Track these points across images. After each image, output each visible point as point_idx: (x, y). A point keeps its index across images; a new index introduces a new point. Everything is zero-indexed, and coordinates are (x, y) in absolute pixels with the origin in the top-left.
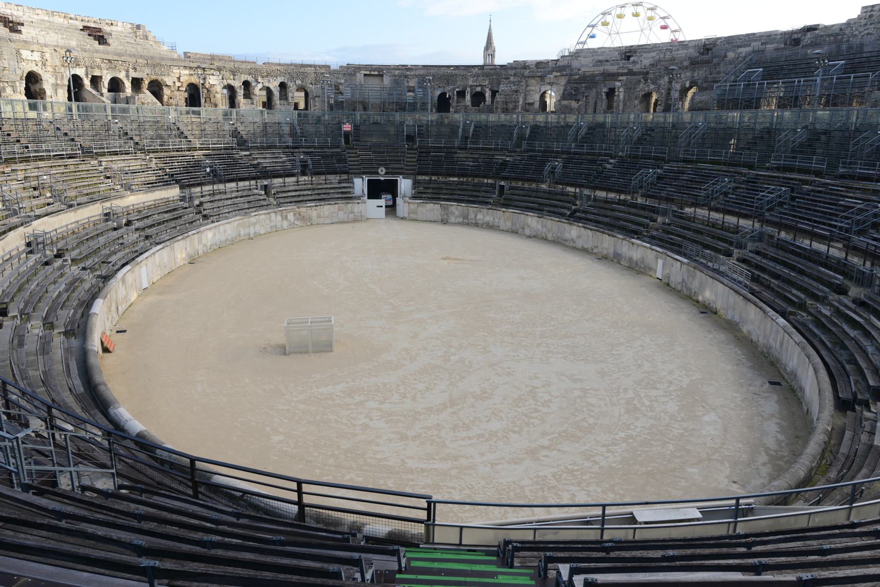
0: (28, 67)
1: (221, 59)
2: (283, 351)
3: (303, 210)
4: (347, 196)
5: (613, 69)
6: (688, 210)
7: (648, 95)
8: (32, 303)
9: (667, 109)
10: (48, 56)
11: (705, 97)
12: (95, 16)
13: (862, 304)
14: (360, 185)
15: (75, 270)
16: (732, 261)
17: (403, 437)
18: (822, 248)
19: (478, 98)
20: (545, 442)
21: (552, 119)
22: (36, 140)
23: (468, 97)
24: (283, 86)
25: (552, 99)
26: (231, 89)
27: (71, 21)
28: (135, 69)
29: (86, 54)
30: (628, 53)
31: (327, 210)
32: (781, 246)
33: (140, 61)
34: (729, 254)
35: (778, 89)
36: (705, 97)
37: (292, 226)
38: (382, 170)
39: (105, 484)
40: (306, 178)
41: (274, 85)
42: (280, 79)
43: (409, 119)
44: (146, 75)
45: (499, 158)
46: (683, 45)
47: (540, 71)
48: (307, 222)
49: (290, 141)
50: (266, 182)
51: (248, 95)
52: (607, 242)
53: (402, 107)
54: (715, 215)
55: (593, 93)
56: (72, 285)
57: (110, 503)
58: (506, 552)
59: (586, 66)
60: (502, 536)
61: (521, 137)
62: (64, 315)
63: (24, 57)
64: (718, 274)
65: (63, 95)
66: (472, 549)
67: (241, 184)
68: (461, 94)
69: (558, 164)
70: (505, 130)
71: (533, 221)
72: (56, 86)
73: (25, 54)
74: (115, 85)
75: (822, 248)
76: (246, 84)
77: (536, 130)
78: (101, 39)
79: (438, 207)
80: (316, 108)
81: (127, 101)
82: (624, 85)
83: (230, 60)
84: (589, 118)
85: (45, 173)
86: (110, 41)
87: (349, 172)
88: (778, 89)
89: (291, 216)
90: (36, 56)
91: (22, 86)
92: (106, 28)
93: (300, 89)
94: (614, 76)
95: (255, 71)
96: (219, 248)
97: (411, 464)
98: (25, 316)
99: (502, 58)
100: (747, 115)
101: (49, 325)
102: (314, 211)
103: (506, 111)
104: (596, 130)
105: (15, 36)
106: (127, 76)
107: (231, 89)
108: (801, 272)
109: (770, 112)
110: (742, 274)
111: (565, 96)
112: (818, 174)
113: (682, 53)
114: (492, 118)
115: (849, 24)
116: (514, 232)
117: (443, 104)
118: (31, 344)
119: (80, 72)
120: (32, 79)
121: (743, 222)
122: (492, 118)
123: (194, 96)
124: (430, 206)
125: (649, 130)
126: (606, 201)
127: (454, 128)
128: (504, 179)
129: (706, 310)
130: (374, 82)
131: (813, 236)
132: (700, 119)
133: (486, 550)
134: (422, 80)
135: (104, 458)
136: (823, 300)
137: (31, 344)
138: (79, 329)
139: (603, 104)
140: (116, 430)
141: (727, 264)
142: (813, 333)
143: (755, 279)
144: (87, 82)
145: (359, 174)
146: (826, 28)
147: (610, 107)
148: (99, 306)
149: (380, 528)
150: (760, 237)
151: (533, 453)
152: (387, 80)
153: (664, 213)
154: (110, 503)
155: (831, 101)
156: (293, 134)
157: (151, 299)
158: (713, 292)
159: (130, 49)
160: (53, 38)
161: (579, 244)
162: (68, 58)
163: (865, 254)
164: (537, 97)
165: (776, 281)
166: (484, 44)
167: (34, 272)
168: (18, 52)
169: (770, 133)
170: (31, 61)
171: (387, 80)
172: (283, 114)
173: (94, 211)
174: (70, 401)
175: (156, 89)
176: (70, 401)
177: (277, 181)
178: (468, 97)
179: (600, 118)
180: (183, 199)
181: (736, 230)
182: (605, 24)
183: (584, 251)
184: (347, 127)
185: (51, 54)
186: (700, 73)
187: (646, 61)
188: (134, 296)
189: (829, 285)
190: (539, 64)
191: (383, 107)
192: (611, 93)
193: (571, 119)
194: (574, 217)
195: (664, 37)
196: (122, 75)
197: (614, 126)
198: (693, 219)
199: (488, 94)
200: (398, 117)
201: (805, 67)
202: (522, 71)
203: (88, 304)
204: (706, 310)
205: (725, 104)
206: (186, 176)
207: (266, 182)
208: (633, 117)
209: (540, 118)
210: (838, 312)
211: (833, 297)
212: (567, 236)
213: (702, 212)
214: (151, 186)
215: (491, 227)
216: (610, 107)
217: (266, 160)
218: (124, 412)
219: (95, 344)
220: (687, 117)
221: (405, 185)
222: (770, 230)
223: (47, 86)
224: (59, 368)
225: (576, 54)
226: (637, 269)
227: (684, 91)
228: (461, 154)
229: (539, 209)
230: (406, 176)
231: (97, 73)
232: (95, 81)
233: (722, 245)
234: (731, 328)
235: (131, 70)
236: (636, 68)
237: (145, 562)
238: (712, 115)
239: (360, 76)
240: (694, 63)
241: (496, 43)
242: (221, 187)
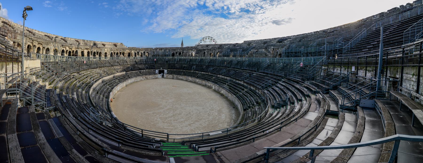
0: (105, 52)
1: (134, 48)
4: (155, 74)
5: (205, 48)
7: (211, 54)
8: (102, 92)
9: (214, 56)
11: (221, 54)
12: (115, 42)
13: (246, 92)
14: (157, 71)
15: (108, 86)
16: (226, 85)
17: (164, 122)
18: (240, 82)
19: (180, 54)
20: (192, 122)
21: (194, 58)
22: (105, 63)
25: (194, 54)
26: (135, 53)
30: (207, 46)
31: (151, 76)
32: (234, 82)
35: (232, 54)
36: (221, 54)
37: (144, 79)
38: (161, 68)
39: (110, 125)
43: (167, 58)
44: (122, 51)
45: (184, 66)
46: (217, 45)
47: (192, 48)
48: (147, 78)
49: (145, 63)
51: (138, 54)
52: (204, 82)
53: (165, 56)
55: (201, 53)
56: (107, 89)
57: (111, 129)
58: (183, 143)
59: (200, 48)
60: (182, 140)
61: (188, 61)
62: (106, 94)
64: (224, 88)
65: (110, 56)
66: (176, 143)
69: (195, 67)
70: (185, 60)
71: (190, 78)
74: (117, 54)
75: (240, 82)
76: (138, 52)
77: (190, 60)
78: (116, 46)
80: (150, 56)
83: (136, 48)
84: (200, 58)
85: (106, 69)
87: (155, 69)
88: (232, 54)
93: (147, 53)
96: (131, 84)
97: (165, 127)
98: (101, 94)
99: (184, 46)
100: (228, 58)
101: (103, 96)
102: (148, 77)
103: (185, 56)
104: (202, 60)
107: (135, 53)
108: (237, 87)
109: (231, 58)
110: (227, 88)
111: (196, 53)
112: (239, 69)
113: (217, 46)
114: (182, 57)
116: (186, 81)
117: (173, 55)
118: (101, 99)
119: (112, 52)
120: (106, 53)
121: (228, 78)
122: (182, 57)
123: (129, 55)
125: (211, 60)
127: (175, 60)
129: (222, 95)
130: (161, 51)
131: (239, 80)
132: (220, 58)
133: (179, 143)
134: (169, 50)
135: (110, 121)
136: (240, 92)
137: (101, 99)
138: (108, 97)
139: (203, 55)
140: (112, 116)
141: (225, 86)
142: (240, 98)
143: (230, 88)
145: (157, 69)
147: (204, 56)
148: (111, 93)
149: (159, 139)
150: (230, 81)
151: (190, 125)
152: (163, 50)
153: (214, 76)
154: (111, 129)
155: (241, 56)
156: (145, 61)
157: (119, 93)
158: (223, 91)
160: (109, 47)
161: (199, 83)
162: (111, 50)
163: (246, 83)
165: (234, 89)
167: (102, 86)
169: (231, 61)
171: (163, 50)
172: (144, 58)
173: (112, 76)
174: (105, 110)
175: (123, 54)
176: (105, 110)
179: (202, 58)
183: (200, 84)
184: (155, 60)
186: (220, 50)
187: (211, 47)
188: (116, 92)
189: (241, 89)
190: (191, 47)
191: (162, 56)
192: (204, 53)
193: (197, 58)
194: (198, 77)
195: (214, 43)
197: (205, 59)
200: (165, 57)
201: (236, 50)
202: (189, 49)
203: (109, 93)
204: (222, 95)
205: (224, 56)
206: (126, 70)
208: (208, 58)
209: (191, 58)
210: (243, 94)
211: (242, 91)
214: (121, 72)
215: (182, 80)
216: (204, 56)
217: (140, 66)
218: (113, 113)
219: (110, 100)
220: (218, 58)
221: (166, 71)
222: (232, 79)
223: (108, 55)
224: (104, 104)
226: (209, 88)
227: (217, 53)
228: (176, 65)
229: (191, 76)
230: (166, 69)
232: (114, 53)
233: (224, 82)
234: (226, 98)
237: (118, 140)
238: (222, 58)
239: (158, 50)
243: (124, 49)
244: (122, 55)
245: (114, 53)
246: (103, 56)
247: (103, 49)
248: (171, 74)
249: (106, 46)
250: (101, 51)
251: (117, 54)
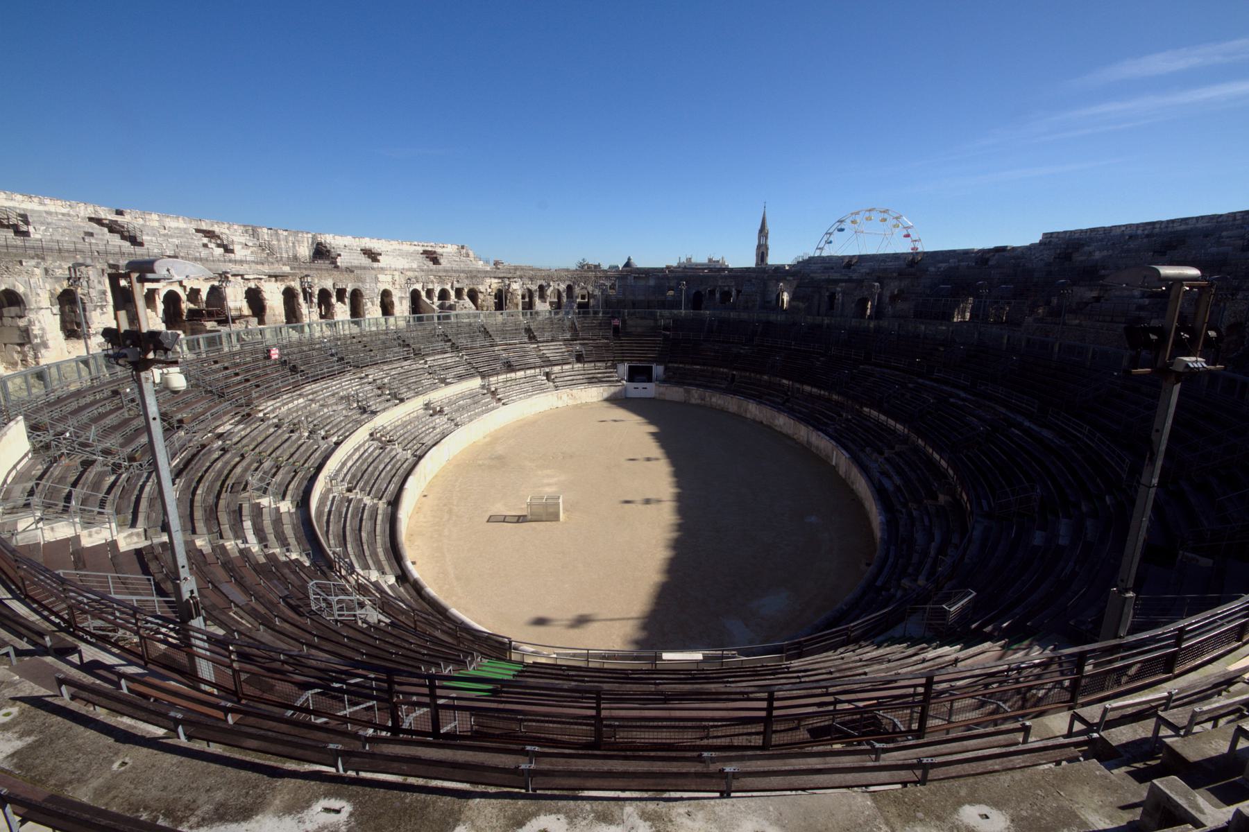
0: (382, 287)
2: (520, 519)
3: (575, 392)
6: (866, 409)
10: (397, 277)
23: (718, 295)
24: (569, 288)
34: (881, 453)
40: (580, 365)
41: (563, 287)
42: (568, 283)
50: (547, 370)
54: (883, 417)
67: (528, 372)
68: (712, 293)
72: (401, 298)
73: (381, 277)
74: (444, 295)
76: (541, 287)
79: (681, 390)
81: (451, 307)
82: (844, 293)
86: (441, 261)
89: (565, 397)
90: (389, 278)
91: (378, 301)
92: (439, 250)
94: (836, 282)
95: (550, 277)
105: (375, 265)
114: (733, 315)
115: (1032, 247)
119: (419, 287)
122: (733, 315)
123: (501, 299)
124: (676, 389)
126: (811, 394)
128: (735, 369)
144: (423, 294)
145: (623, 361)
146: (1014, 249)
159: (455, 266)
160: (402, 263)
164: (774, 296)
166: (759, 227)
168: (377, 278)
170: (385, 282)
175: (473, 295)
177: (557, 369)
178: (718, 295)
180: (483, 387)
181: (893, 432)
182: (854, 222)
187: (864, 270)
196: (448, 287)
198: (868, 418)
199: (734, 293)
207: (547, 370)
212: (777, 422)
213: (874, 413)
223: (395, 300)
225: (811, 260)
230: (659, 363)
231: (430, 286)
232: (429, 293)
236: (855, 276)
240: (901, 274)
241: (769, 226)
242: (513, 375)
243: (474, 275)
244: (467, 301)
245: (429, 293)
246: (373, 311)
247: (368, 276)
248: (679, 383)
249: (384, 261)
250: (359, 285)
251: (444, 295)
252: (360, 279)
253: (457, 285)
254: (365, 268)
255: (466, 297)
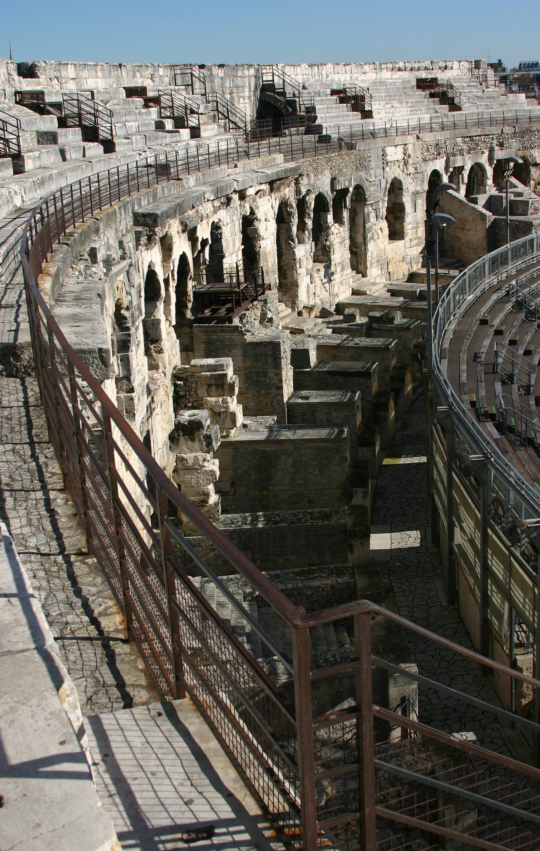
10: (410, 147)
27: (400, 73)
28: (501, 145)
29: (447, 134)
33: (508, 130)
63: (389, 158)
106: (490, 158)
119: (439, 165)
185: (414, 144)
235: (496, 148)
249: (382, 114)
252: (362, 164)
253: (499, 154)
254: (363, 136)
255: (513, 180)
